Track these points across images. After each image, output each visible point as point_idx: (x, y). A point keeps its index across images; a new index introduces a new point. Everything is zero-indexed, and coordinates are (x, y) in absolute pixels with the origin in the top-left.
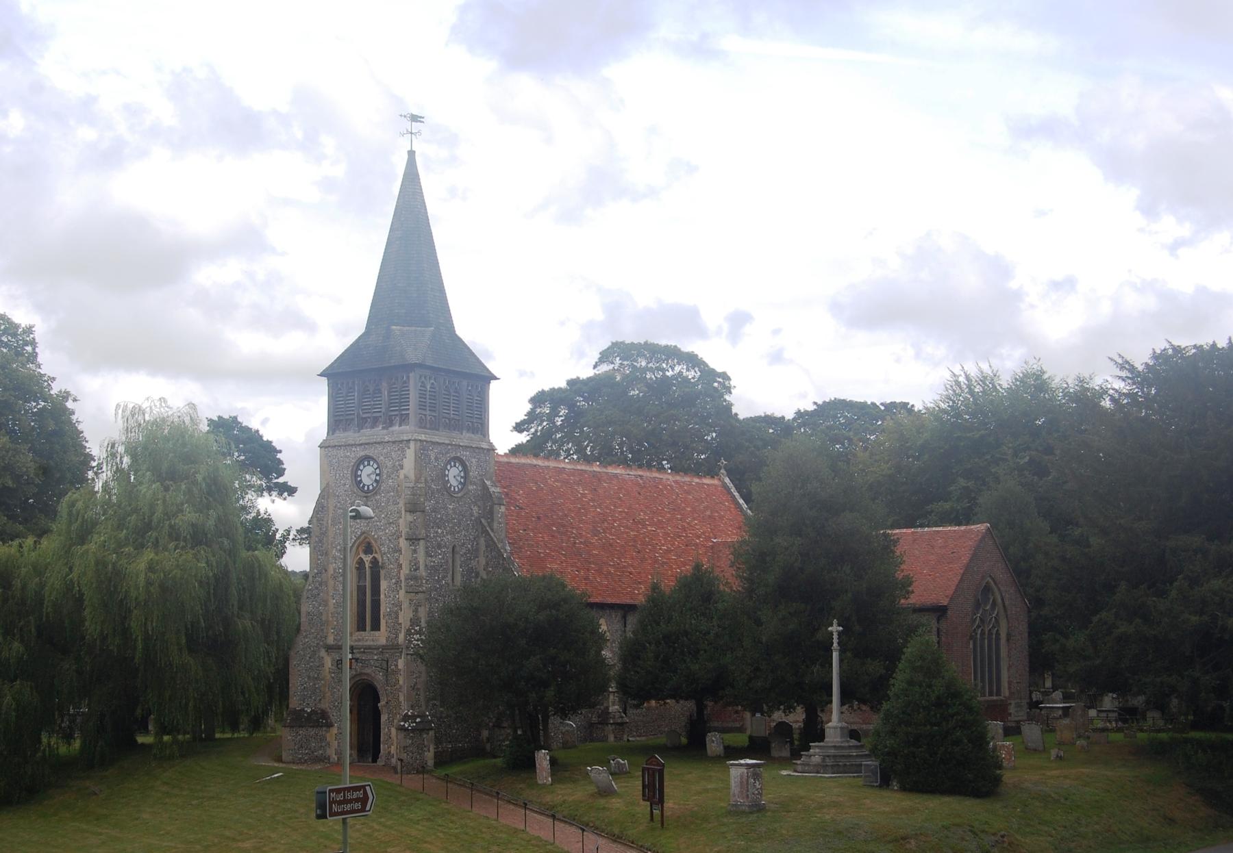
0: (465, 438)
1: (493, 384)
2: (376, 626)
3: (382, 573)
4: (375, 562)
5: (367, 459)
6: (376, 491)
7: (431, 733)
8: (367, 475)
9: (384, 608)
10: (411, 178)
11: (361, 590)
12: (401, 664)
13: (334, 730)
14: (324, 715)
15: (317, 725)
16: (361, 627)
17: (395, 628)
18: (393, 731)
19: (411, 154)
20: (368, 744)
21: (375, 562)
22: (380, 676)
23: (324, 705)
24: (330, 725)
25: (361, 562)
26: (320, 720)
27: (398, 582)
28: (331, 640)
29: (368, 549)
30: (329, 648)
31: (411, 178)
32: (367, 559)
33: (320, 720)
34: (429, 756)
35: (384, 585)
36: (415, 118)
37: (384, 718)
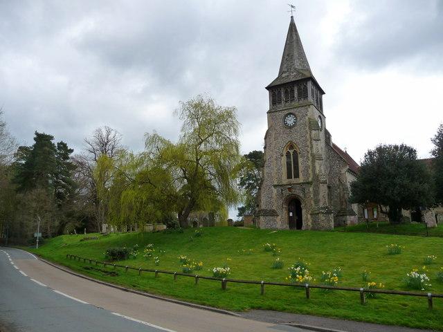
2: (297, 176)
3: (299, 155)
4: (295, 153)
5: (290, 114)
7: (332, 215)
10: (293, 28)
11: (289, 164)
12: (311, 189)
13: (279, 217)
14: (274, 211)
15: (274, 216)
16: (289, 177)
17: (307, 175)
18: (309, 216)
19: (292, 17)
20: (296, 223)
21: (295, 153)
22: (301, 195)
25: (288, 154)
27: (308, 158)
28: (276, 183)
29: (291, 147)
30: (275, 186)
31: (293, 28)
32: (291, 152)
33: (273, 213)
34: (332, 224)
35: (300, 160)
36: (292, 6)
37: (304, 211)
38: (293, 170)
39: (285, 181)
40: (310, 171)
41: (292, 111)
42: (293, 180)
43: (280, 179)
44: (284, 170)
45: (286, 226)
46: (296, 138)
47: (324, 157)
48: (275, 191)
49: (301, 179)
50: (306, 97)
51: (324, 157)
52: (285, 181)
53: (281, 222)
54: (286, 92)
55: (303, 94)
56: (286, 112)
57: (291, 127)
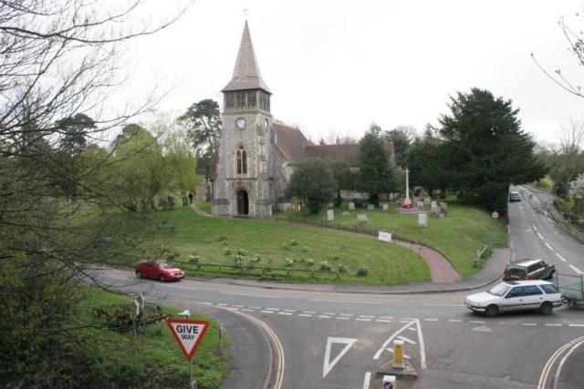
0: (267, 113)
1: (272, 97)
2: (245, 172)
3: (247, 155)
4: (244, 152)
5: (241, 118)
6: (245, 129)
8: (241, 124)
9: (249, 166)
11: (239, 161)
12: (256, 184)
16: (239, 172)
17: (253, 172)
19: (246, 22)
21: (244, 152)
22: (248, 188)
23: (227, 197)
24: (229, 204)
25: (239, 152)
26: (226, 202)
28: (228, 177)
29: (241, 147)
33: (226, 202)
35: (248, 159)
37: (250, 201)
38: (242, 167)
39: (235, 175)
40: (256, 169)
41: (241, 116)
42: (242, 175)
43: (231, 174)
44: (235, 167)
45: (236, 213)
46: (245, 139)
47: (267, 158)
48: (227, 183)
49: (248, 175)
50: (254, 105)
51: (267, 158)
52: (235, 175)
53: (232, 208)
54: (238, 97)
55: (253, 102)
56: (238, 116)
57: (241, 130)
